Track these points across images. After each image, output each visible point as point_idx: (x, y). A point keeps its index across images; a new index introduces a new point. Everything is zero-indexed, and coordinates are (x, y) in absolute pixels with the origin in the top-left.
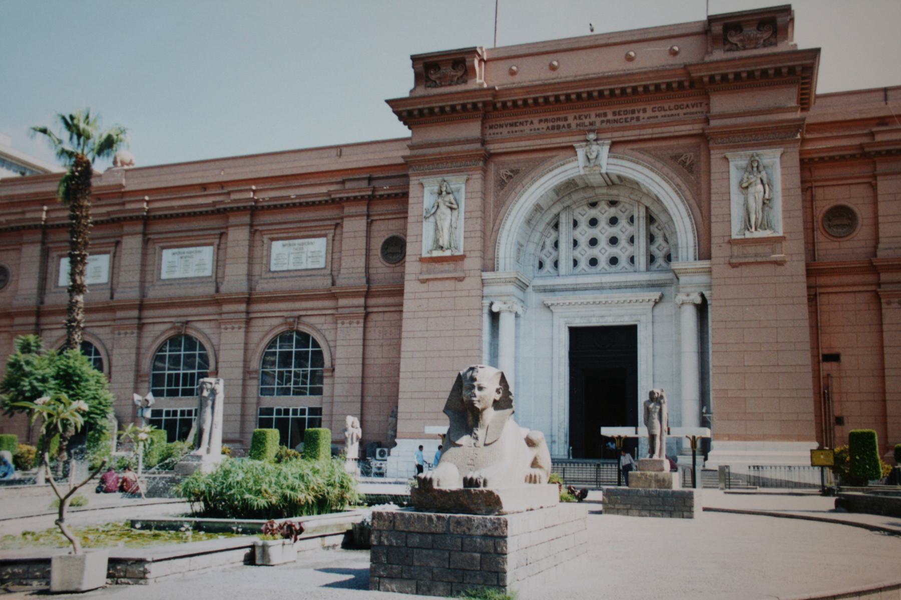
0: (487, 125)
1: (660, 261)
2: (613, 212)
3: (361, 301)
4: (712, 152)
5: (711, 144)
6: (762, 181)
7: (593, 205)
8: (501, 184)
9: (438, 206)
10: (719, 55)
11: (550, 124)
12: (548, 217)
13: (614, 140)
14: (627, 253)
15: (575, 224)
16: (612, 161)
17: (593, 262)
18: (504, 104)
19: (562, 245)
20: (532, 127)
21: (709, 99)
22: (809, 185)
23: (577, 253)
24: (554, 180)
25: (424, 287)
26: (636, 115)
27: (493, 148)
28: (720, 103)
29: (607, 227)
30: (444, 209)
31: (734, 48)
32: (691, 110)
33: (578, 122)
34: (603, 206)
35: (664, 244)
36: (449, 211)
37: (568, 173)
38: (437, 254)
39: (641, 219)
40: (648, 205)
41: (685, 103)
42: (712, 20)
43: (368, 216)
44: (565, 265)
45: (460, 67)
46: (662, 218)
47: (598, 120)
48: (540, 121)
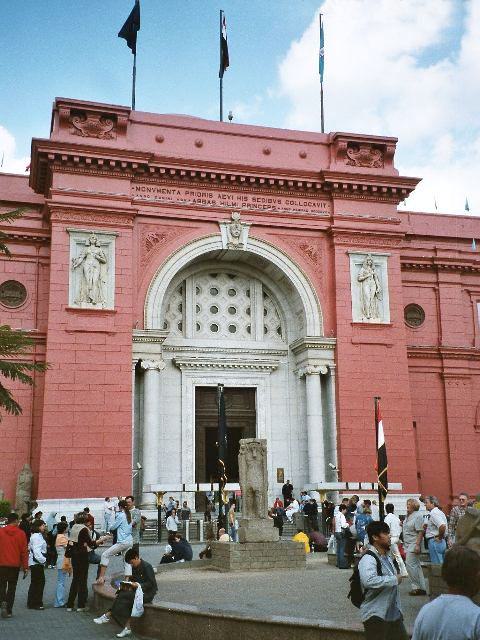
0: (135, 185)
1: (273, 333)
2: (231, 284)
4: (336, 248)
5: (335, 241)
7: (214, 276)
8: (149, 245)
10: (340, 166)
12: (178, 283)
15: (198, 291)
17: (215, 328)
18: (157, 170)
23: (200, 318)
28: (344, 207)
29: (227, 297)
30: (91, 261)
31: (352, 163)
32: (316, 208)
33: (223, 201)
38: (85, 306)
40: (265, 282)
41: (313, 201)
42: (337, 137)
44: (190, 326)
47: (240, 203)
48: (187, 193)
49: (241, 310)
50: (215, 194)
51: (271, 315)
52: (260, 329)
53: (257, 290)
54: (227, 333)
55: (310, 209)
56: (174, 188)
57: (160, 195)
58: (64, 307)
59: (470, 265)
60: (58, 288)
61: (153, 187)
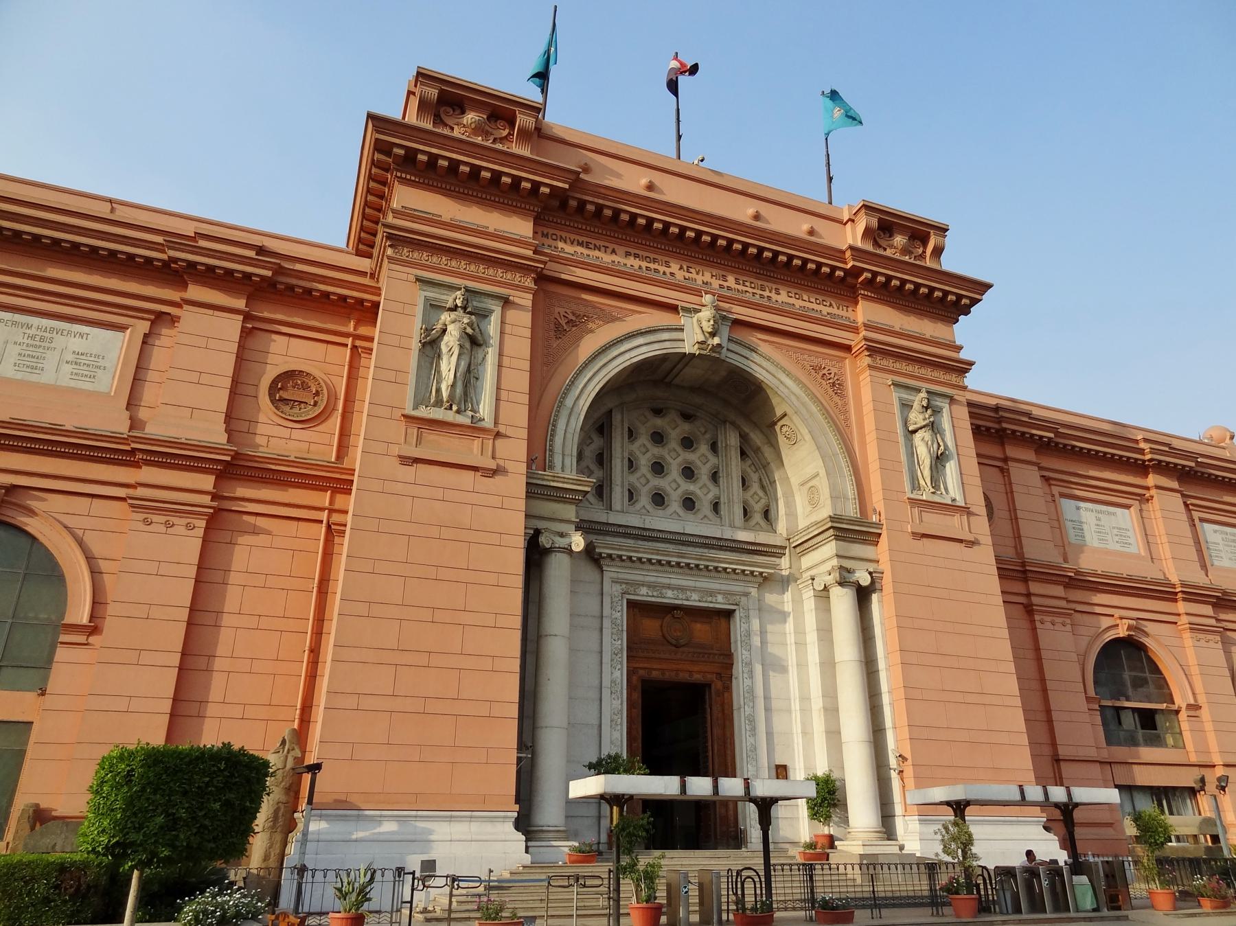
0: (540, 229)
1: (758, 518)
2: (685, 428)
3: (207, 482)
7: (658, 412)
8: (559, 331)
9: (444, 331)
11: (644, 264)
14: (710, 496)
17: (659, 499)
18: (582, 204)
19: (618, 465)
20: (616, 258)
21: (857, 303)
23: (633, 479)
24: (644, 349)
25: (409, 472)
26: (766, 293)
27: (555, 269)
29: (679, 449)
32: (835, 311)
33: (687, 275)
34: (673, 415)
35: (761, 493)
36: (468, 345)
37: (667, 345)
39: (733, 452)
40: (747, 430)
41: (829, 300)
43: (247, 317)
45: (500, 123)
46: (767, 452)
47: (716, 283)
48: (628, 254)
49: (704, 472)
51: (755, 487)
52: (739, 511)
53: (733, 440)
54: (681, 511)
55: (825, 310)
56: (606, 244)
57: (585, 251)
58: (397, 414)
59: (1052, 435)
60: (391, 376)
61: (573, 237)
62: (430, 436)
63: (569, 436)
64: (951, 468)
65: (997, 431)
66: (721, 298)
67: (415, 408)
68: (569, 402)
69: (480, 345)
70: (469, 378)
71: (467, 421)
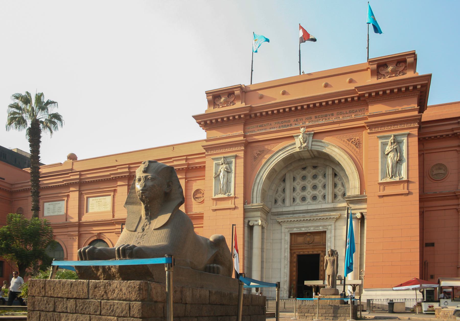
0: (247, 127)
6: (396, 150)
8: (255, 158)
12: (281, 175)
13: (315, 132)
16: (314, 143)
18: (256, 114)
20: (271, 126)
22: (422, 152)
27: (250, 139)
45: (232, 96)
50: (292, 120)
56: (267, 123)
62: (218, 202)
63: (258, 191)
64: (404, 166)
65: (453, 134)
66: (308, 127)
67: (215, 196)
68: (258, 181)
69: (230, 172)
70: (228, 183)
71: (227, 196)
